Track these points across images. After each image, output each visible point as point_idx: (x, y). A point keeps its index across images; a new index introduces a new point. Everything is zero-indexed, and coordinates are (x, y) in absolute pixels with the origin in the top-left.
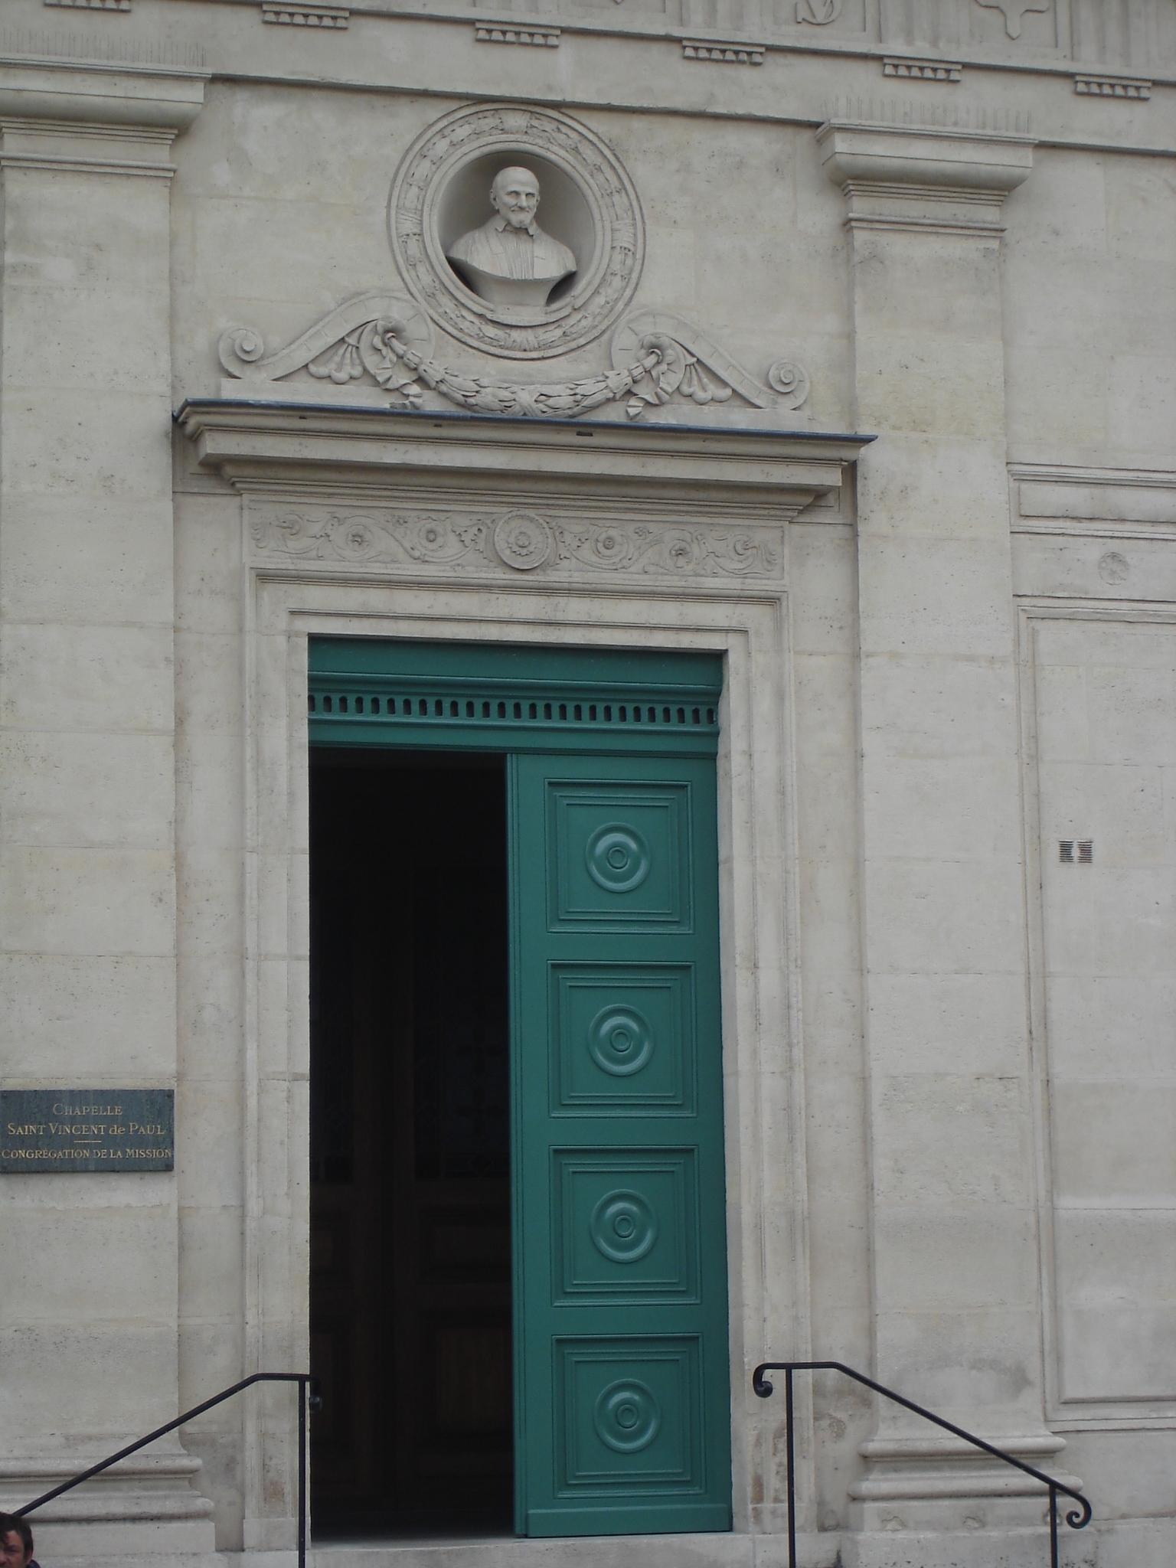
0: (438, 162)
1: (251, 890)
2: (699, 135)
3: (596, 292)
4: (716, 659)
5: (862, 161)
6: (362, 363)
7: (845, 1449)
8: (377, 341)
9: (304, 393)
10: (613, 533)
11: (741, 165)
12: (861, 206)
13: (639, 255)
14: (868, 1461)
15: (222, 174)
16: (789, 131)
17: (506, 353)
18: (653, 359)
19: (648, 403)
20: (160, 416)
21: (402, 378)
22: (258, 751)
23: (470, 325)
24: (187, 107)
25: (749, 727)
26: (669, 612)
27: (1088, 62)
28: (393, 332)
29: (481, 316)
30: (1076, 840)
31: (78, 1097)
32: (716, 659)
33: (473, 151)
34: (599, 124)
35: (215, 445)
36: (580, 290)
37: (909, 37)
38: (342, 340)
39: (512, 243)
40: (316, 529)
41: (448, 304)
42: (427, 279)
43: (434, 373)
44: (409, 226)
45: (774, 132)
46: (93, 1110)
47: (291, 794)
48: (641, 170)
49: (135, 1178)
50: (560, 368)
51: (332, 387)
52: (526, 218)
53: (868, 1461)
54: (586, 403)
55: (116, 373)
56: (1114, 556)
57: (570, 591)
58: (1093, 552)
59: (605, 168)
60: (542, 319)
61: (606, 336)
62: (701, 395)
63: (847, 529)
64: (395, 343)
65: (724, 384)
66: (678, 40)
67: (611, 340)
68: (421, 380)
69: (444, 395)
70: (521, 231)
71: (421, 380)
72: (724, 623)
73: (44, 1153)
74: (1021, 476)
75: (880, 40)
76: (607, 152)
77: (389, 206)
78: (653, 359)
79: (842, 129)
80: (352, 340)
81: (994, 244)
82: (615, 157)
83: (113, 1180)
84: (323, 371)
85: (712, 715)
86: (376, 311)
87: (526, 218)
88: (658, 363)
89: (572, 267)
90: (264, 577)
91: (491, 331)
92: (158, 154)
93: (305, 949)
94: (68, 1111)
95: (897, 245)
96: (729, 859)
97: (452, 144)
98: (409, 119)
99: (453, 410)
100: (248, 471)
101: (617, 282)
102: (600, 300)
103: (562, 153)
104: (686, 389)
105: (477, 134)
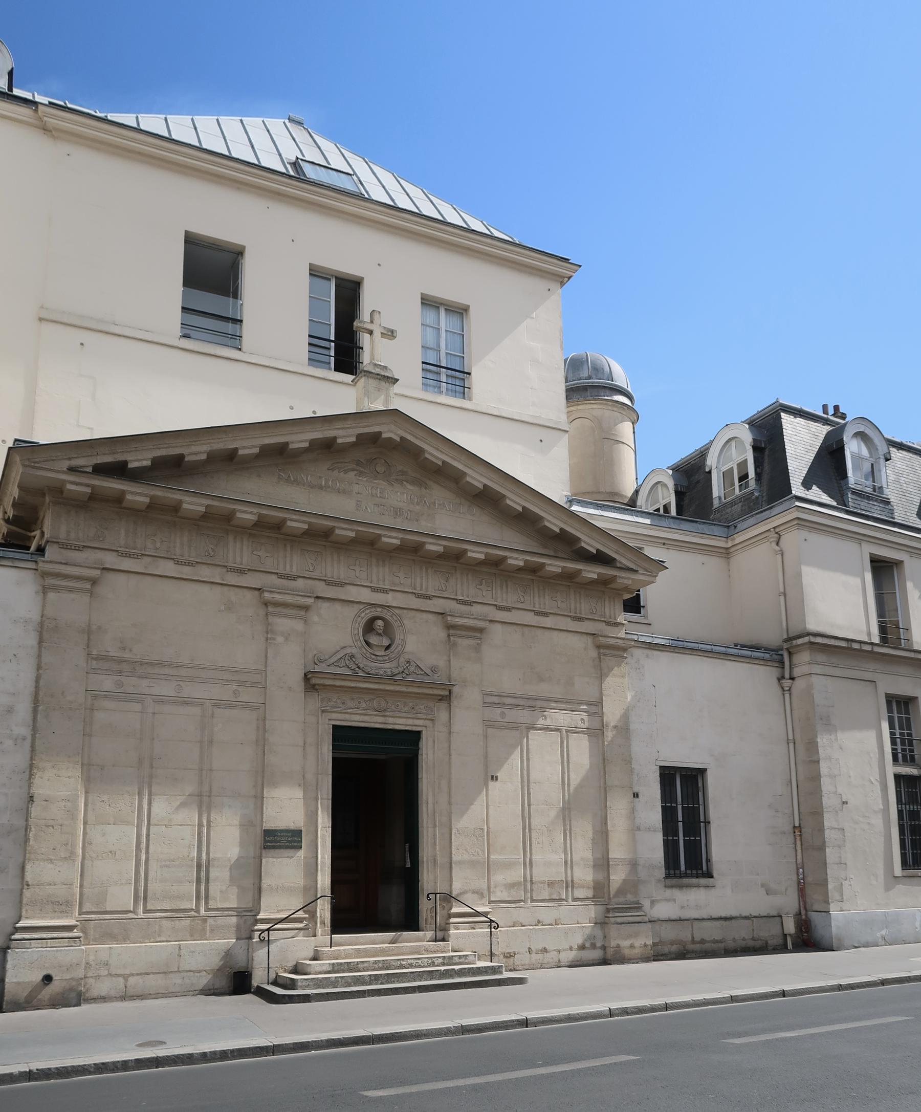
0: (362, 618)
1: (319, 784)
2: (418, 614)
3: (396, 648)
4: (418, 733)
5: (453, 622)
6: (346, 663)
9: (333, 670)
10: (398, 703)
11: (427, 622)
12: (452, 632)
16: (437, 615)
18: (408, 664)
19: (407, 674)
22: (321, 752)
24: (309, 603)
25: (427, 748)
27: (499, 603)
28: (352, 656)
29: (371, 653)
31: (281, 831)
32: (418, 733)
33: (370, 616)
34: (397, 611)
35: (314, 681)
36: (393, 648)
38: (341, 658)
41: (364, 651)
42: (360, 644)
43: (361, 666)
44: (356, 632)
45: (433, 615)
46: (285, 834)
47: (328, 762)
48: (406, 622)
49: (293, 850)
50: (387, 665)
52: (381, 632)
54: (394, 674)
55: (292, 663)
56: (503, 712)
58: (499, 711)
59: (399, 622)
60: (384, 654)
61: (397, 659)
62: (418, 673)
63: (448, 704)
64: (353, 659)
65: (423, 671)
67: (399, 660)
68: (358, 667)
69: (363, 671)
70: (380, 634)
71: (358, 667)
73: (274, 844)
74: (485, 694)
75: (456, 595)
77: (352, 627)
78: (408, 664)
79: (449, 615)
80: (344, 658)
81: (479, 642)
83: (288, 850)
84: (337, 665)
85: (418, 745)
86: (349, 651)
87: (381, 632)
88: (409, 665)
91: (373, 657)
93: (330, 797)
94: (279, 834)
95: (459, 641)
96: (422, 778)
97: (365, 614)
98: (357, 608)
100: (321, 687)
101: (400, 647)
102: (397, 650)
104: (414, 672)
105: (371, 612)
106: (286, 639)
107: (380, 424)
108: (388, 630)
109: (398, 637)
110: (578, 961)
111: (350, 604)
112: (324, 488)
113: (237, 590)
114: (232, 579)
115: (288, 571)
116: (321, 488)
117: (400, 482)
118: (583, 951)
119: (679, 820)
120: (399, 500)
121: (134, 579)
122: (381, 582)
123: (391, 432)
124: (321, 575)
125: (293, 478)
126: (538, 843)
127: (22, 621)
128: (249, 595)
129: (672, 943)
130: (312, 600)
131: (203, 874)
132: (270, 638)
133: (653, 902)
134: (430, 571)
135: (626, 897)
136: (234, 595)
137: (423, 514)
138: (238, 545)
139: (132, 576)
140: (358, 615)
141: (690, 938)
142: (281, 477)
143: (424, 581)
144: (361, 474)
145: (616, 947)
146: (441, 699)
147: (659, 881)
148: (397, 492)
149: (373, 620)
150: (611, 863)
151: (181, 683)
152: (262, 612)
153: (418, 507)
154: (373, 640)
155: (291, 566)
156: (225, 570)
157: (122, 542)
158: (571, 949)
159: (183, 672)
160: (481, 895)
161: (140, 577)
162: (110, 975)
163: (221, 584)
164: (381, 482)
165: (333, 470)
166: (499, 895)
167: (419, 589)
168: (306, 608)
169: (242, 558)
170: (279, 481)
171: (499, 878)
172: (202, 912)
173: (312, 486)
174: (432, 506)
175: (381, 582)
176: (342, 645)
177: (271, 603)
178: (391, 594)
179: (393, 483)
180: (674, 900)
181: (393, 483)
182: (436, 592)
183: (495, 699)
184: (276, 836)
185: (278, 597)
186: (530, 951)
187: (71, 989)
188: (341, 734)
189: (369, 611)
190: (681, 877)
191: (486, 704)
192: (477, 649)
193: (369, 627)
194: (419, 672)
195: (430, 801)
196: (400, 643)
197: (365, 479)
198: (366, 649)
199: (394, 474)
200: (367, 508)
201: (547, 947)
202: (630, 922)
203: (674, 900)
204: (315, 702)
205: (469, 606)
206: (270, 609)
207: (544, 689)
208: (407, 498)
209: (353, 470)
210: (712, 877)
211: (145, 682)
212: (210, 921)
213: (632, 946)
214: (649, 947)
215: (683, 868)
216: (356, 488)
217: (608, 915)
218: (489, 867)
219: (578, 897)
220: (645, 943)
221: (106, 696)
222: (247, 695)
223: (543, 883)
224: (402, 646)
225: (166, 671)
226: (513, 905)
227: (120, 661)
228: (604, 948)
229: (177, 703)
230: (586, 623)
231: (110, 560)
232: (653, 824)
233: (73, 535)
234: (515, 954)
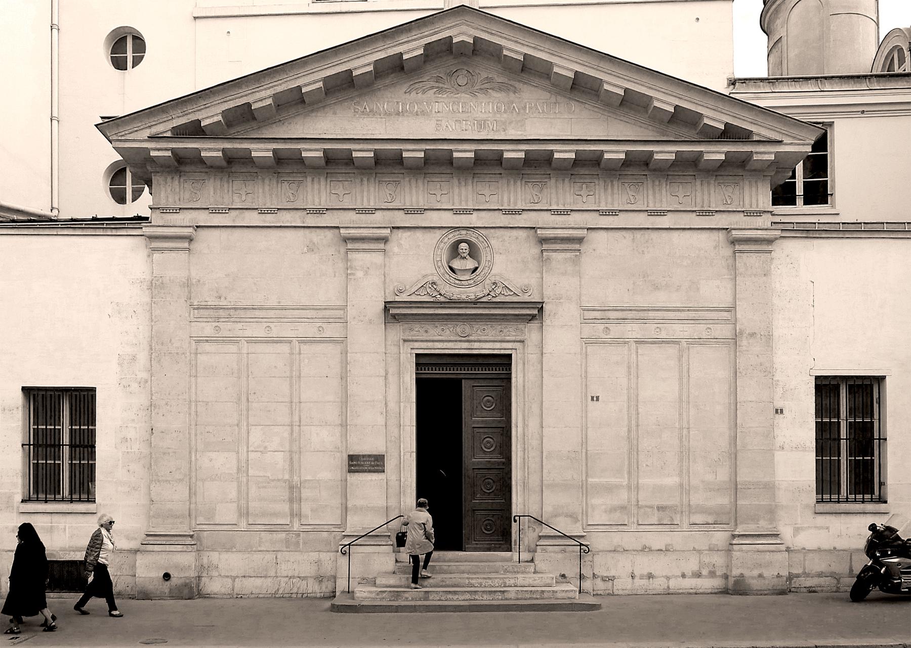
2: (507, 233)
7: (535, 535)
8: (430, 286)
14: (540, 537)
15: (396, 249)
16: (529, 229)
20: (382, 306)
23: (452, 280)
26: (498, 345)
28: (434, 283)
30: (595, 395)
33: (453, 240)
34: (483, 231)
35: (392, 311)
37: (558, 205)
39: (462, 261)
40: (417, 329)
44: (438, 259)
45: (525, 230)
48: (493, 242)
51: (420, 297)
53: (540, 537)
56: (607, 328)
57: (475, 341)
58: (602, 327)
60: (469, 278)
62: (506, 294)
66: (501, 210)
68: (440, 294)
71: (440, 294)
72: (511, 347)
75: (551, 205)
81: (578, 253)
82: (487, 239)
86: (430, 279)
87: (465, 255)
90: (405, 341)
91: (457, 282)
92: (382, 246)
95: (554, 255)
98: (438, 233)
99: (448, 301)
101: (487, 268)
104: (502, 293)
106: (366, 273)
107: (449, 28)
108: (474, 253)
109: (484, 256)
111: (431, 230)
112: (401, 114)
113: (318, 230)
114: (311, 220)
115: (366, 205)
116: (398, 114)
117: (485, 91)
120: (483, 111)
121: (224, 233)
122: (463, 203)
123: (463, 34)
124: (400, 204)
125: (369, 109)
127: (138, 281)
128: (329, 234)
130: (388, 231)
132: (350, 274)
134: (519, 183)
135: (758, 524)
136: (316, 236)
137: (510, 123)
138: (316, 186)
139: (223, 229)
140: (441, 241)
142: (357, 110)
143: (512, 195)
144: (440, 90)
146: (533, 317)
147: (807, 506)
148: (481, 103)
149: (455, 247)
150: (739, 486)
152: (343, 250)
153: (505, 115)
154: (456, 264)
155: (369, 201)
157: (212, 200)
159: (272, 313)
161: (229, 230)
163: (304, 227)
164: (463, 95)
165: (410, 92)
167: (506, 204)
168: (385, 240)
169: (320, 198)
170: (355, 115)
173: (388, 114)
174: (522, 111)
175: (463, 203)
176: (424, 273)
177: (349, 239)
178: (475, 213)
179: (476, 94)
181: (476, 94)
182: (528, 205)
183: (597, 314)
185: (353, 233)
188: (422, 361)
189: (452, 235)
190: (839, 502)
191: (585, 321)
192: (576, 261)
193: (454, 251)
195: (520, 425)
196: (487, 265)
197: (445, 96)
198: (450, 276)
199: (477, 85)
200: (447, 127)
204: (397, 332)
205: (568, 216)
206: (350, 246)
207: (661, 299)
208: (493, 108)
209: (432, 88)
210: (886, 502)
211: (240, 326)
213: (760, 576)
214: (785, 579)
216: (436, 107)
217: (734, 542)
218: (585, 489)
221: (207, 341)
222: (332, 331)
224: (489, 267)
225: (257, 313)
227: (216, 308)
228: (726, 577)
229: (267, 342)
231: (203, 218)
232: (802, 443)
233: (170, 200)
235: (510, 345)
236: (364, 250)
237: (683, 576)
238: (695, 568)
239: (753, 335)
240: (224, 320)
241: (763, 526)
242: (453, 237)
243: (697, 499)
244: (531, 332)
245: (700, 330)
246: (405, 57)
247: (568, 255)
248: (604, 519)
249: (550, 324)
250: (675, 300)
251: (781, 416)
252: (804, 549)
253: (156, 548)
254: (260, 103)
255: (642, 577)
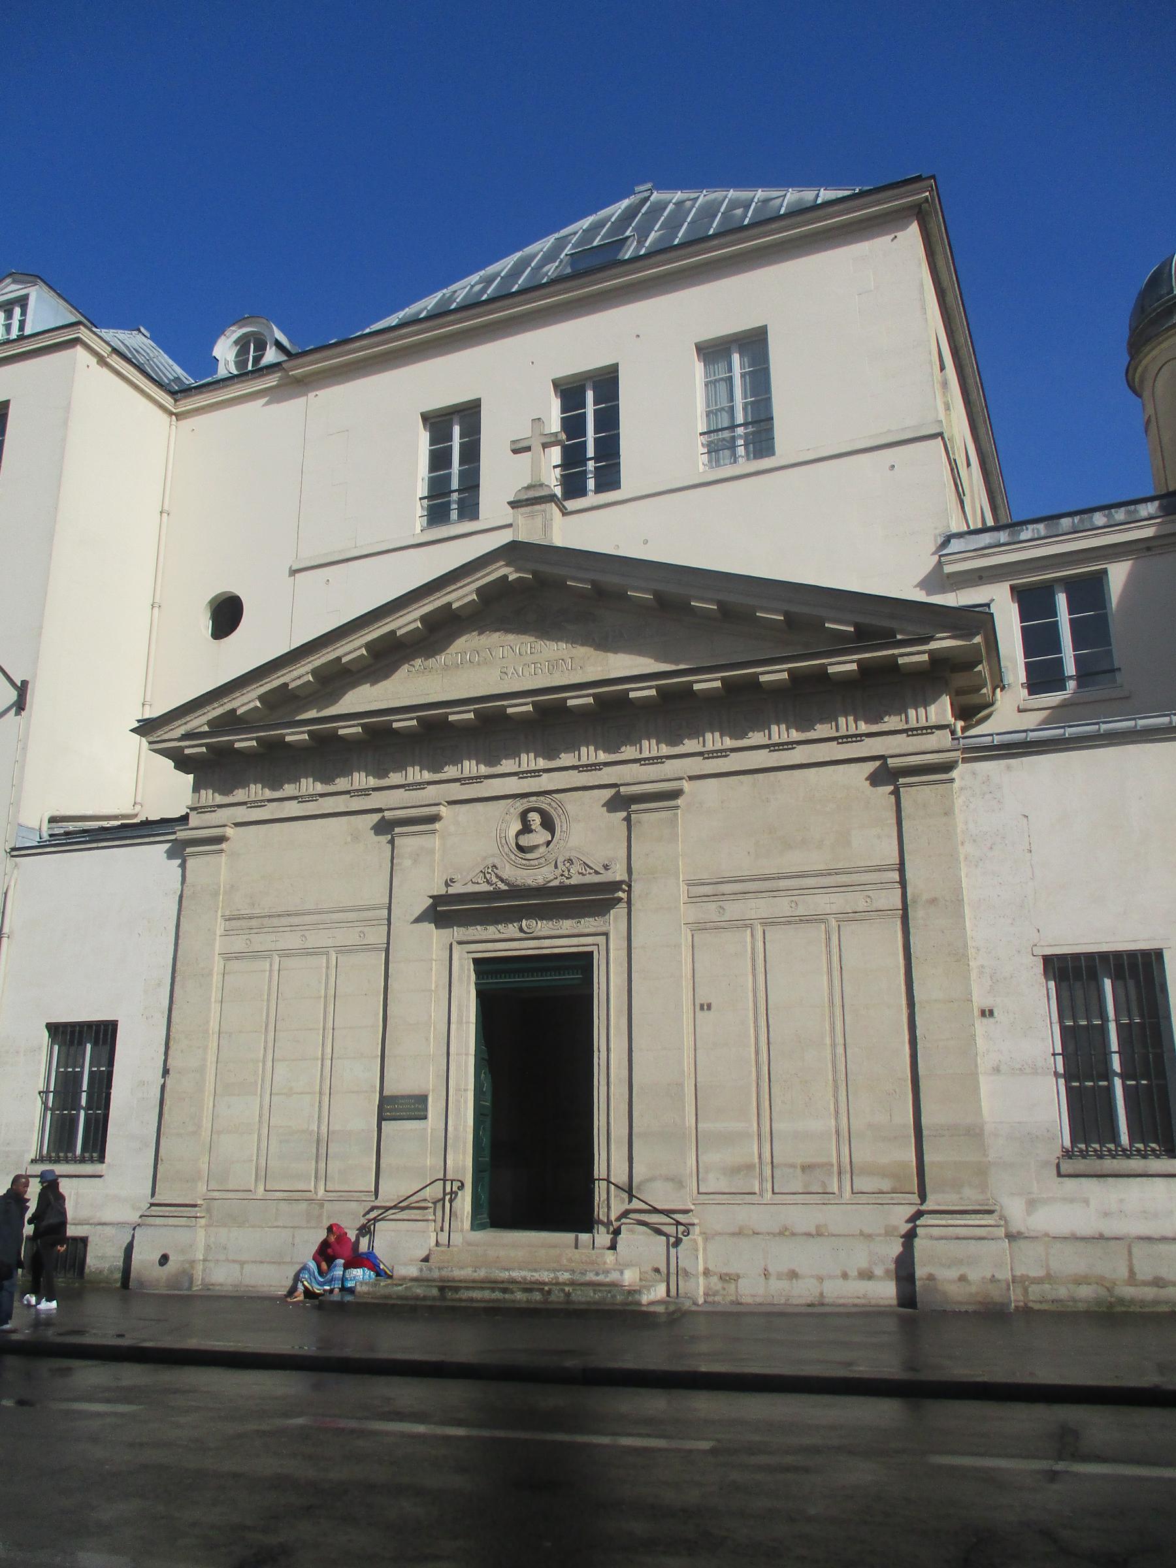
13: (568, 832)
17: (529, 868)
21: (494, 880)
30: (705, 1001)
31: (403, 1097)
48: (570, 808)
54: (547, 880)
58: (713, 906)
72: (591, 943)
76: (558, 802)
82: (561, 805)
86: (490, 862)
89: (550, 839)
91: (524, 862)
95: (645, 817)
103: (546, 805)
110: (859, 1298)
112: (461, 666)
118: (870, 1282)
119: (1113, 1050)
126: (783, 1102)
129: (1079, 1281)
131: (323, 1151)
133: (1032, 1204)
141: (1123, 1272)
145: (928, 1279)
151: (303, 933)
156: (348, 796)
158: (845, 1276)
159: (307, 919)
160: (679, 1183)
162: (227, 1260)
166: (713, 1183)
171: (711, 1157)
172: (321, 1192)
173: (446, 667)
178: (545, 776)
180: (1086, 1202)
184: (398, 1104)
186: (766, 1275)
187: (184, 1272)
194: (586, 870)
201: (797, 1270)
202: (960, 1236)
203: (1086, 1202)
207: (795, 861)
211: (273, 937)
212: (326, 1204)
213: (963, 1278)
215: (1124, 1139)
219: (859, 1191)
220: (994, 1276)
223: (793, 1166)
226: (738, 1199)
229: (302, 955)
230: (868, 741)
234: (739, 1277)
235: (589, 940)
236: (414, 834)
237: (845, 1276)
238: (864, 1264)
239: (933, 901)
240: (255, 931)
241: (970, 1197)
242: (521, 805)
243: (864, 1154)
244: (615, 920)
245: (859, 901)
246: (454, 606)
247: (664, 814)
248: (723, 1185)
249: (640, 908)
250: (815, 860)
251: (991, 1020)
252: (1047, 1235)
253: (158, 1221)
254: (298, 680)
255: (779, 1277)
